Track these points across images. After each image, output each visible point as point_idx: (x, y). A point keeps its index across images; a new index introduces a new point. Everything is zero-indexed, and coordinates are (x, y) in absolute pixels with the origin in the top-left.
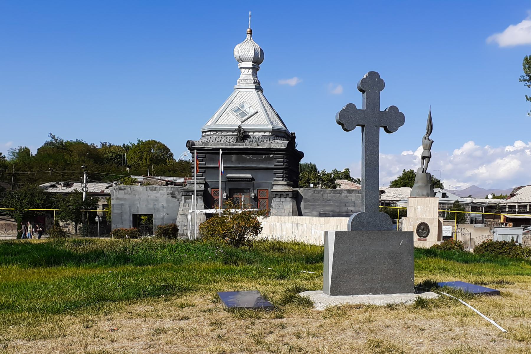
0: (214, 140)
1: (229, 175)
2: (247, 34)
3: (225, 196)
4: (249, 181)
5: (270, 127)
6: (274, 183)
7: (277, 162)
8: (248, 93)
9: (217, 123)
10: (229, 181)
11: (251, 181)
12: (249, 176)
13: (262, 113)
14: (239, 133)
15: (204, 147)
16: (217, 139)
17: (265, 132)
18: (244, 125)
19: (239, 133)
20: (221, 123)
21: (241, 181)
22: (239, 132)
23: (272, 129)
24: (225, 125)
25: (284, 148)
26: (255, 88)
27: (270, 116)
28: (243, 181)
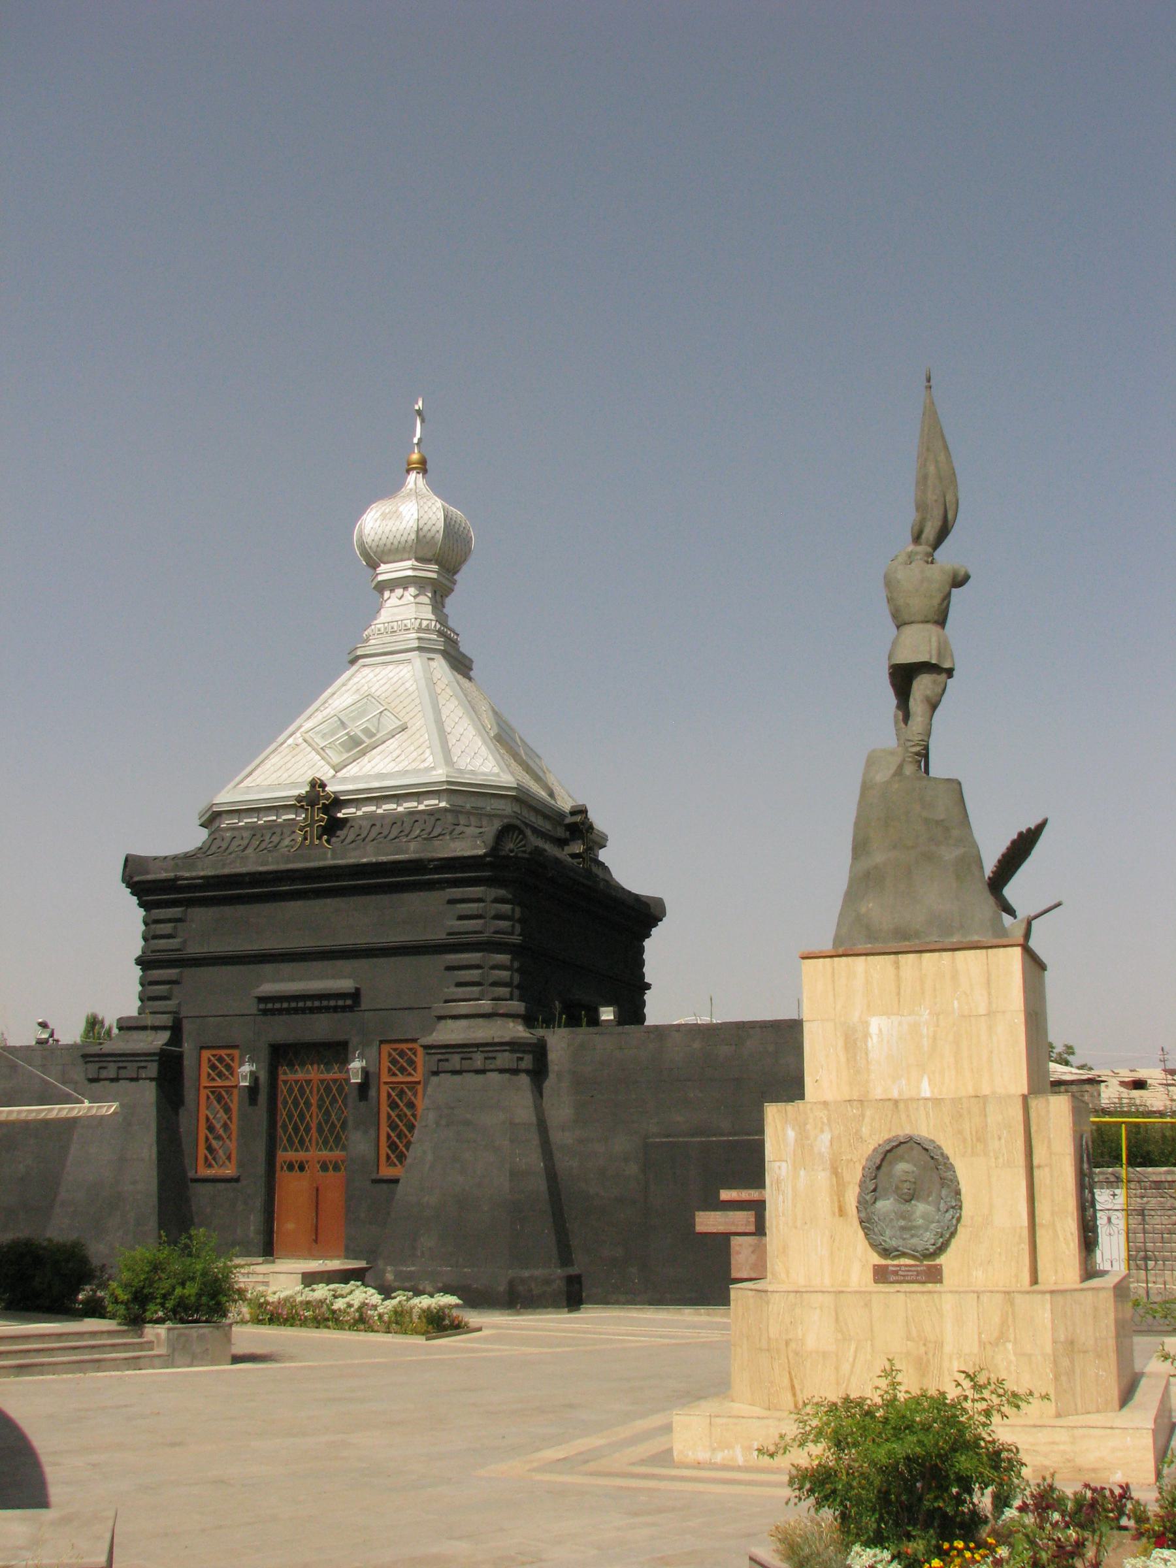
0: (224, 845)
1: (269, 988)
2: (408, 471)
3: (245, 1077)
4: (344, 1009)
5: (440, 774)
6: (440, 1008)
7: (461, 918)
8: (390, 667)
9: (246, 783)
10: (265, 1012)
11: (350, 1009)
12: (345, 984)
13: (424, 730)
14: (313, 811)
15: (177, 879)
16: (235, 843)
17: (418, 796)
18: (344, 780)
19: (313, 811)
20: (258, 782)
21: (312, 1010)
22: (313, 807)
23: (449, 783)
24: (270, 787)
25: (481, 852)
26: (419, 649)
27: (452, 740)
28: (319, 1010)
